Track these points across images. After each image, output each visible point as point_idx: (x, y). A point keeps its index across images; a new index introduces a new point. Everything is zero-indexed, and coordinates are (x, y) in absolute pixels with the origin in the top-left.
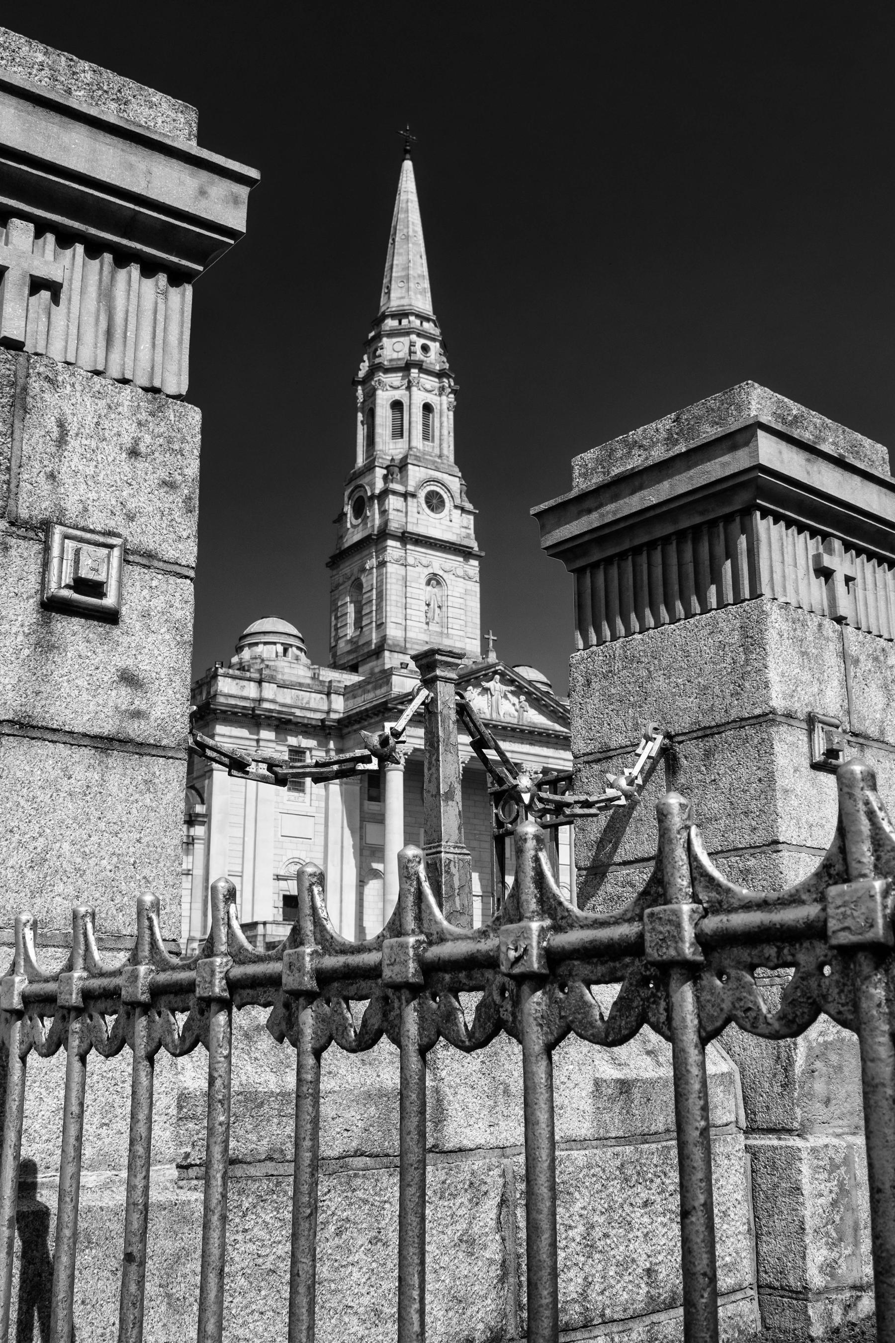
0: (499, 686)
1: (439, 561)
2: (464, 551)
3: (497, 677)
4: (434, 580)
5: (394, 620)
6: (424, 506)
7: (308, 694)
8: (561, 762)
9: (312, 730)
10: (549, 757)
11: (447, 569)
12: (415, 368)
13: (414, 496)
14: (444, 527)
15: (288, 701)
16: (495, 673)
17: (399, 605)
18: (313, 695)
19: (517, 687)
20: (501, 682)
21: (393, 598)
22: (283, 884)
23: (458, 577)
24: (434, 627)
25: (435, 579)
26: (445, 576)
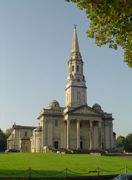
1: (79, 89)
4: (79, 92)
16: (85, 107)
20: (86, 108)
24: (79, 100)
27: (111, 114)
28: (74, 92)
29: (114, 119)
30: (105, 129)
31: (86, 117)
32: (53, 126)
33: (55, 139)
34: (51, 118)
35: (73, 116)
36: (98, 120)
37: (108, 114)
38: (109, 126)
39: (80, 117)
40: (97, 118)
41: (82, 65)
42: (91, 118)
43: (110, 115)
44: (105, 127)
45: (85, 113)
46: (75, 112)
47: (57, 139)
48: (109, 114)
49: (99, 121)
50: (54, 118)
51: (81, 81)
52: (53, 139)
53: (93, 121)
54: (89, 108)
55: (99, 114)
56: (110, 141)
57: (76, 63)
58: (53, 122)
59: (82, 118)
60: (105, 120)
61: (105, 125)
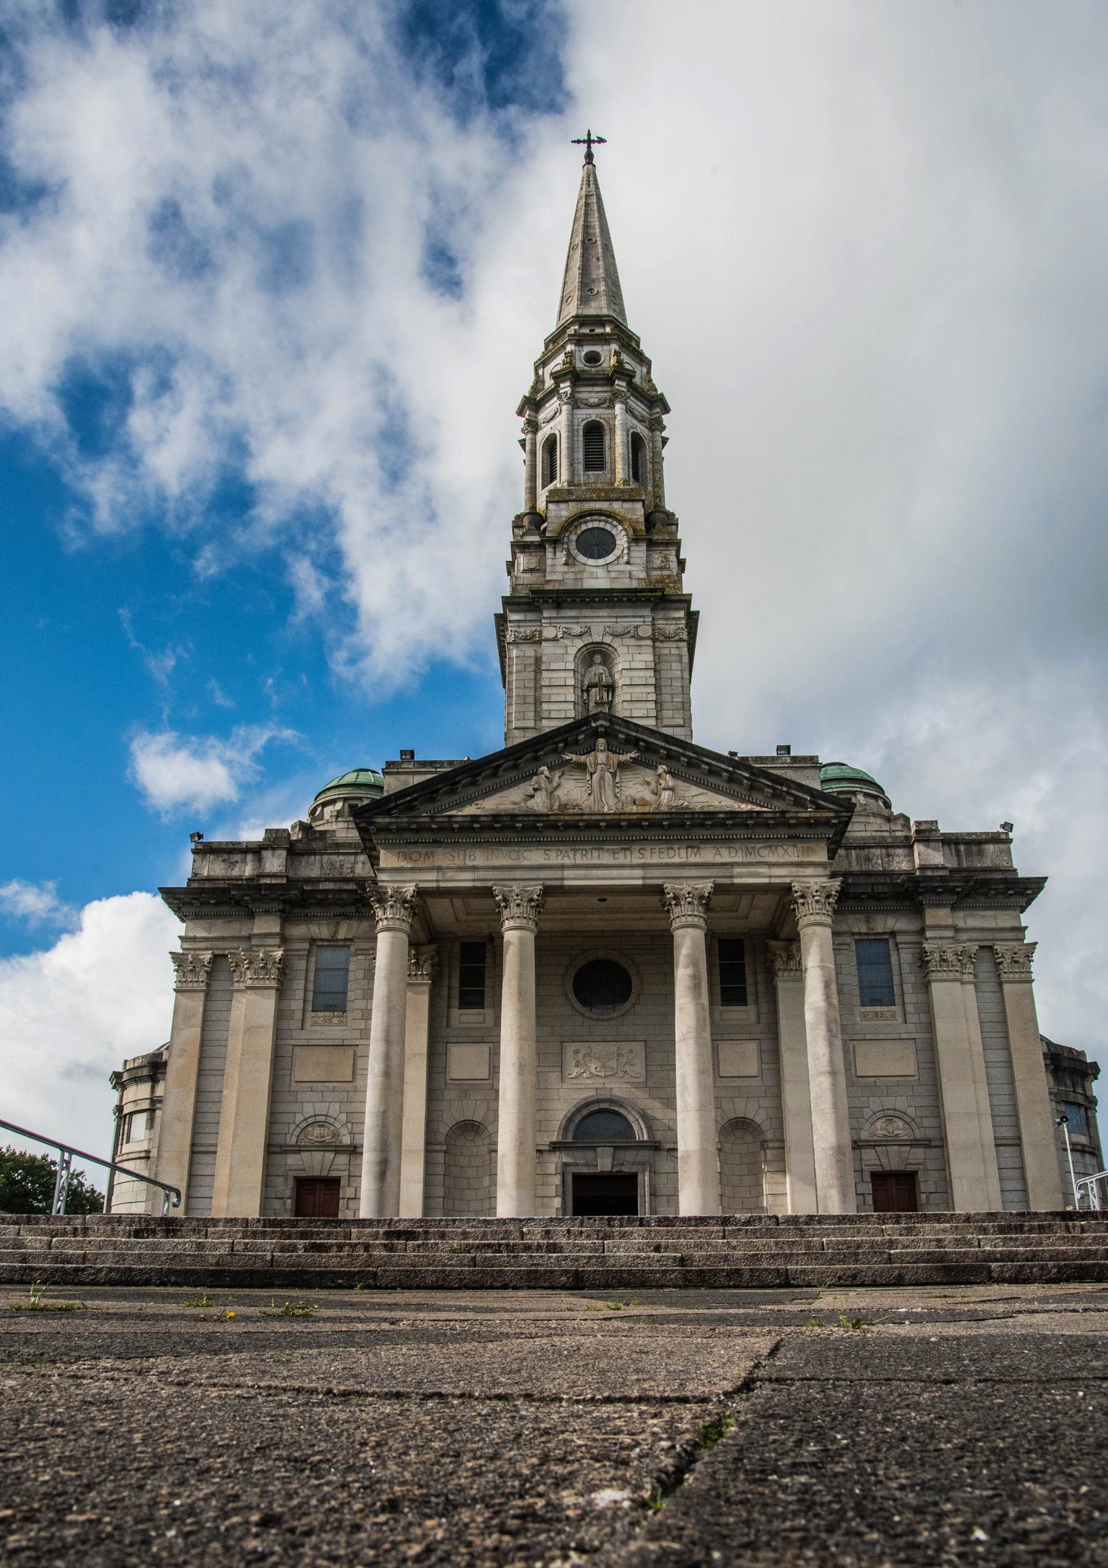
0: (601, 757)
2: (648, 599)
3: (601, 742)
6: (575, 552)
8: (764, 870)
9: (353, 909)
10: (732, 865)
11: (619, 629)
12: (564, 381)
13: (556, 542)
14: (613, 575)
15: (315, 873)
16: (596, 734)
17: (531, 700)
19: (639, 750)
20: (609, 749)
22: (292, 1159)
23: (642, 638)
25: (600, 652)
26: (616, 643)
27: (1001, 839)
28: (538, 660)
29: (1036, 885)
30: (928, 1009)
31: (622, 859)
32: (280, 1015)
33: (298, 1149)
34: (267, 925)
35: (443, 858)
36: (780, 876)
37: (951, 841)
38: (985, 967)
39: (535, 857)
41: (656, 425)
42: (680, 855)
43: (990, 848)
44: (926, 986)
45: (609, 805)
46: (470, 810)
47: (324, 1147)
48: (975, 842)
49: (796, 886)
50: (299, 930)
51: (622, 541)
52: (273, 1149)
53: (707, 886)
54: (650, 748)
55: (779, 805)
56: (999, 1144)
57: (575, 403)
58: (284, 970)
59: (563, 867)
60: (918, 911)
61: (922, 962)
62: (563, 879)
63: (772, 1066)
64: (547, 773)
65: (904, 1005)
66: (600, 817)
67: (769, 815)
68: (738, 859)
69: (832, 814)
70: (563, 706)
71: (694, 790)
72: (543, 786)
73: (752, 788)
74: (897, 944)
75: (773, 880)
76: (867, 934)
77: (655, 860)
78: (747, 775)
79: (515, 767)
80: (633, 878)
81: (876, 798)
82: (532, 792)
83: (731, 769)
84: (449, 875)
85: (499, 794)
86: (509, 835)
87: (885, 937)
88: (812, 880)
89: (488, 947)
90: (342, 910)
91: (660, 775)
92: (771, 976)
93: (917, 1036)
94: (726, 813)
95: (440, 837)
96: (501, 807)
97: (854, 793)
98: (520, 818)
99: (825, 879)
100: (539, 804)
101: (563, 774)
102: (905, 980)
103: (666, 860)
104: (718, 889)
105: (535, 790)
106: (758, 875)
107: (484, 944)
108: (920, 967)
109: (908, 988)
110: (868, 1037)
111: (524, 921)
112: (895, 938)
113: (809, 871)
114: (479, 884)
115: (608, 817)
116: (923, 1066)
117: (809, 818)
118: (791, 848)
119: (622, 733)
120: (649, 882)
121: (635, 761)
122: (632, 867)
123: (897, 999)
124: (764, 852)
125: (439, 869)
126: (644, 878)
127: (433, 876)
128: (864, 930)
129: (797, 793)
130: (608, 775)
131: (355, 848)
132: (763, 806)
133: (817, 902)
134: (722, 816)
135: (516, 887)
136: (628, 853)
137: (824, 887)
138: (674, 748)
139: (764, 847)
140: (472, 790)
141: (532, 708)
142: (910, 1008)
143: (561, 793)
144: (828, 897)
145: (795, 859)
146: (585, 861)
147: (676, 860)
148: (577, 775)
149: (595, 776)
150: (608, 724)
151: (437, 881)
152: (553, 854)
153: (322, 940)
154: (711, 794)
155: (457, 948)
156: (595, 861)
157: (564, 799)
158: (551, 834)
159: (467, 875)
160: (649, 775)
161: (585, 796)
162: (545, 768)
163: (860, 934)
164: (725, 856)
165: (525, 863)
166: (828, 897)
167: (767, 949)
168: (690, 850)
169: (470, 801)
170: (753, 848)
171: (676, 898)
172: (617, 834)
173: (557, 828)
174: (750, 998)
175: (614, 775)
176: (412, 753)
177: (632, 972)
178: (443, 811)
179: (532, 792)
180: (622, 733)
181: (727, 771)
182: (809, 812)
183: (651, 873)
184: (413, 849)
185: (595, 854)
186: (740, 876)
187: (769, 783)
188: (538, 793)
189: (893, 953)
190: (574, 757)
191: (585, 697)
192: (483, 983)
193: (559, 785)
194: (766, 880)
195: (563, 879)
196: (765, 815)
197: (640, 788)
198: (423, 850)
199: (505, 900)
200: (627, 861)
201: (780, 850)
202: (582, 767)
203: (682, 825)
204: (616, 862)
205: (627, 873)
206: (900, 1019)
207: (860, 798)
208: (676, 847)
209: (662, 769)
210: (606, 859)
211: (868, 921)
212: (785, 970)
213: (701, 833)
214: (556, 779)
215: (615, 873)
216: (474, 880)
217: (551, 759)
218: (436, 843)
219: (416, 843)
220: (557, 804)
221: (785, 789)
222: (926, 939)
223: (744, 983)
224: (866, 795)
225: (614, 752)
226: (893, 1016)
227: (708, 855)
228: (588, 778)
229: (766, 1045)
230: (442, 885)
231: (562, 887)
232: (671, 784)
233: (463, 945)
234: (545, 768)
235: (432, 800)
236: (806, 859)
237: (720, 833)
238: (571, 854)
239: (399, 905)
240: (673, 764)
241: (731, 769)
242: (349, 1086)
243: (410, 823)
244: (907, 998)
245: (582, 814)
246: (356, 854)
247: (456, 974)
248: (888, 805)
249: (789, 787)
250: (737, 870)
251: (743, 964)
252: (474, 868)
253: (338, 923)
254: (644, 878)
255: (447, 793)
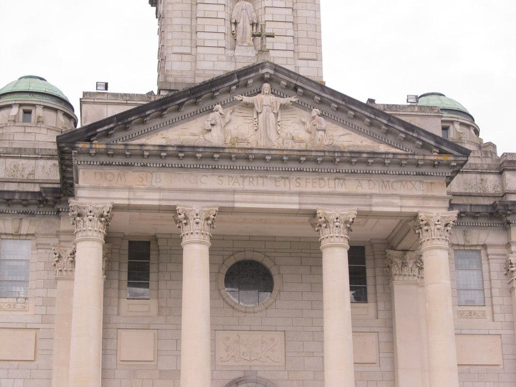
3: (266, 86)
5: (177, 50)
7: (33, 162)
8: (397, 201)
10: (371, 195)
16: (263, 80)
17: (188, 29)
18: (41, 162)
21: (176, 21)
31: (283, 186)
35: (133, 177)
36: (409, 206)
39: (210, 181)
40: (400, 189)
42: (329, 185)
46: (155, 140)
49: (422, 216)
55: (410, 147)
59: (234, 192)
62: (233, 202)
63: (388, 355)
64: (221, 110)
65: (492, 306)
66: (266, 152)
67: (403, 157)
68: (376, 191)
69: (451, 158)
70: (215, 36)
71: (341, 131)
72: (218, 121)
73: (387, 132)
74: (487, 256)
75: (404, 210)
76: (464, 246)
77: (309, 188)
78: (385, 122)
79: (195, 104)
80: (291, 203)
81: (468, 126)
82: (210, 127)
83: (372, 116)
84: (139, 194)
85: (180, 126)
86: (189, 162)
87: (478, 248)
88: (434, 212)
89: (152, 246)
90: (25, 209)
91: (314, 118)
92: (388, 278)
93: (502, 332)
94: (368, 153)
95: (129, 161)
96: (182, 137)
97: (452, 122)
98: (201, 150)
99: (445, 211)
100: (216, 138)
101: (233, 111)
102: (493, 285)
103: (317, 189)
104: (360, 214)
105: (212, 125)
106: (392, 205)
107: (148, 243)
108: (506, 274)
109: (495, 292)
110: (463, 332)
111: (202, 237)
112: (486, 249)
113: (432, 203)
114: (164, 203)
115: (273, 152)
116: (506, 357)
117: (434, 161)
118: (418, 183)
119: (284, 80)
120: (304, 207)
121: (294, 103)
122: (291, 194)
123: (488, 301)
124: (397, 186)
125: (130, 189)
126: (300, 204)
127: (125, 194)
128: (462, 242)
129: (424, 139)
130: (272, 116)
131: (35, 153)
132: (396, 147)
133: (438, 229)
134: (365, 155)
135: (196, 208)
136: (287, 181)
137: (444, 217)
138: (326, 96)
139: (397, 181)
140: (158, 122)
141: (189, 36)
142: (497, 309)
143: (230, 127)
144: (446, 225)
145: (420, 193)
146: (252, 187)
147: (326, 189)
148: (246, 112)
149: (261, 116)
150: (272, 72)
151: (129, 199)
152: (225, 180)
153: (6, 234)
154: (354, 135)
155: (125, 246)
156: (261, 188)
157: (235, 133)
158: (225, 163)
159: (156, 195)
160: (304, 115)
161: (252, 131)
162: (219, 106)
163: (458, 245)
164: (365, 187)
165: (203, 186)
166: (446, 225)
167: (384, 256)
168: (337, 181)
169: (155, 130)
170: (388, 182)
171: (326, 222)
172: (278, 165)
173: (230, 158)
174: (370, 297)
175: (276, 115)
176: (106, 85)
177: (274, 271)
178: (133, 138)
179: (210, 127)
180: (284, 80)
181: (369, 118)
182: (434, 157)
183: (306, 199)
184: (107, 169)
185: (260, 181)
186: (377, 205)
187: (403, 130)
188: (214, 129)
189: (484, 262)
190: (246, 99)
191: (233, 29)
192: (148, 277)
193: (230, 121)
194: (398, 210)
195: (233, 202)
196: (399, 157)
197: (297, 126)
198: (115, 171)
199: (186, 218)
200: (286, 189)
201: (409, 184)
202: (251, 106)
203: (333, 161)
204: (278, 189)
205: (286, 198)
206: (489, 317)
207: (457, 126)
208: (326, 178)
209: (316, 112)
210: (269, 185)
211: (465, 235)
212: (400, 275)
213: (347, 167)
214: (228, 116)
215: (276, 198)
216: (160, 200)
217: (225, 98)
218: (127, 165)
219: (110, 164)
220: (229, 137)
221: (415, 135)
222: (512, 253)
223: (366, 284)
224: (462, 124)
225: (276, 95)
226: (484, 314)
227: (351, 186)
228: (255, 116)
229: (384, 337)
230: (133, 202)
231: (233, 208)
232: (323, 126)
233: (130, 242)
234: (219, 106)
235: (126, 129)
236: (429, 194)
237: (361, 168)
238: (240, 180)
239: (96, 219)
240: (325, 108)
241: (372, 116)
242: (33, 364)
243: (107, 150)
244: (496, 300)
245: (252, 149)
246: (36, 158)
247: (125, 268)
248: (477, 132)
249: (418, 134)
250: (375, 200)
251: (364, 268)
252: (160, 190)
253: (21, 219)
254: (300, 204)
255: (138, 124)
